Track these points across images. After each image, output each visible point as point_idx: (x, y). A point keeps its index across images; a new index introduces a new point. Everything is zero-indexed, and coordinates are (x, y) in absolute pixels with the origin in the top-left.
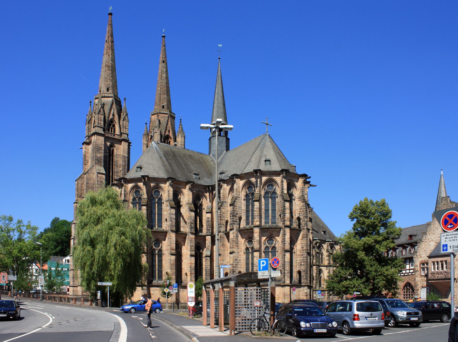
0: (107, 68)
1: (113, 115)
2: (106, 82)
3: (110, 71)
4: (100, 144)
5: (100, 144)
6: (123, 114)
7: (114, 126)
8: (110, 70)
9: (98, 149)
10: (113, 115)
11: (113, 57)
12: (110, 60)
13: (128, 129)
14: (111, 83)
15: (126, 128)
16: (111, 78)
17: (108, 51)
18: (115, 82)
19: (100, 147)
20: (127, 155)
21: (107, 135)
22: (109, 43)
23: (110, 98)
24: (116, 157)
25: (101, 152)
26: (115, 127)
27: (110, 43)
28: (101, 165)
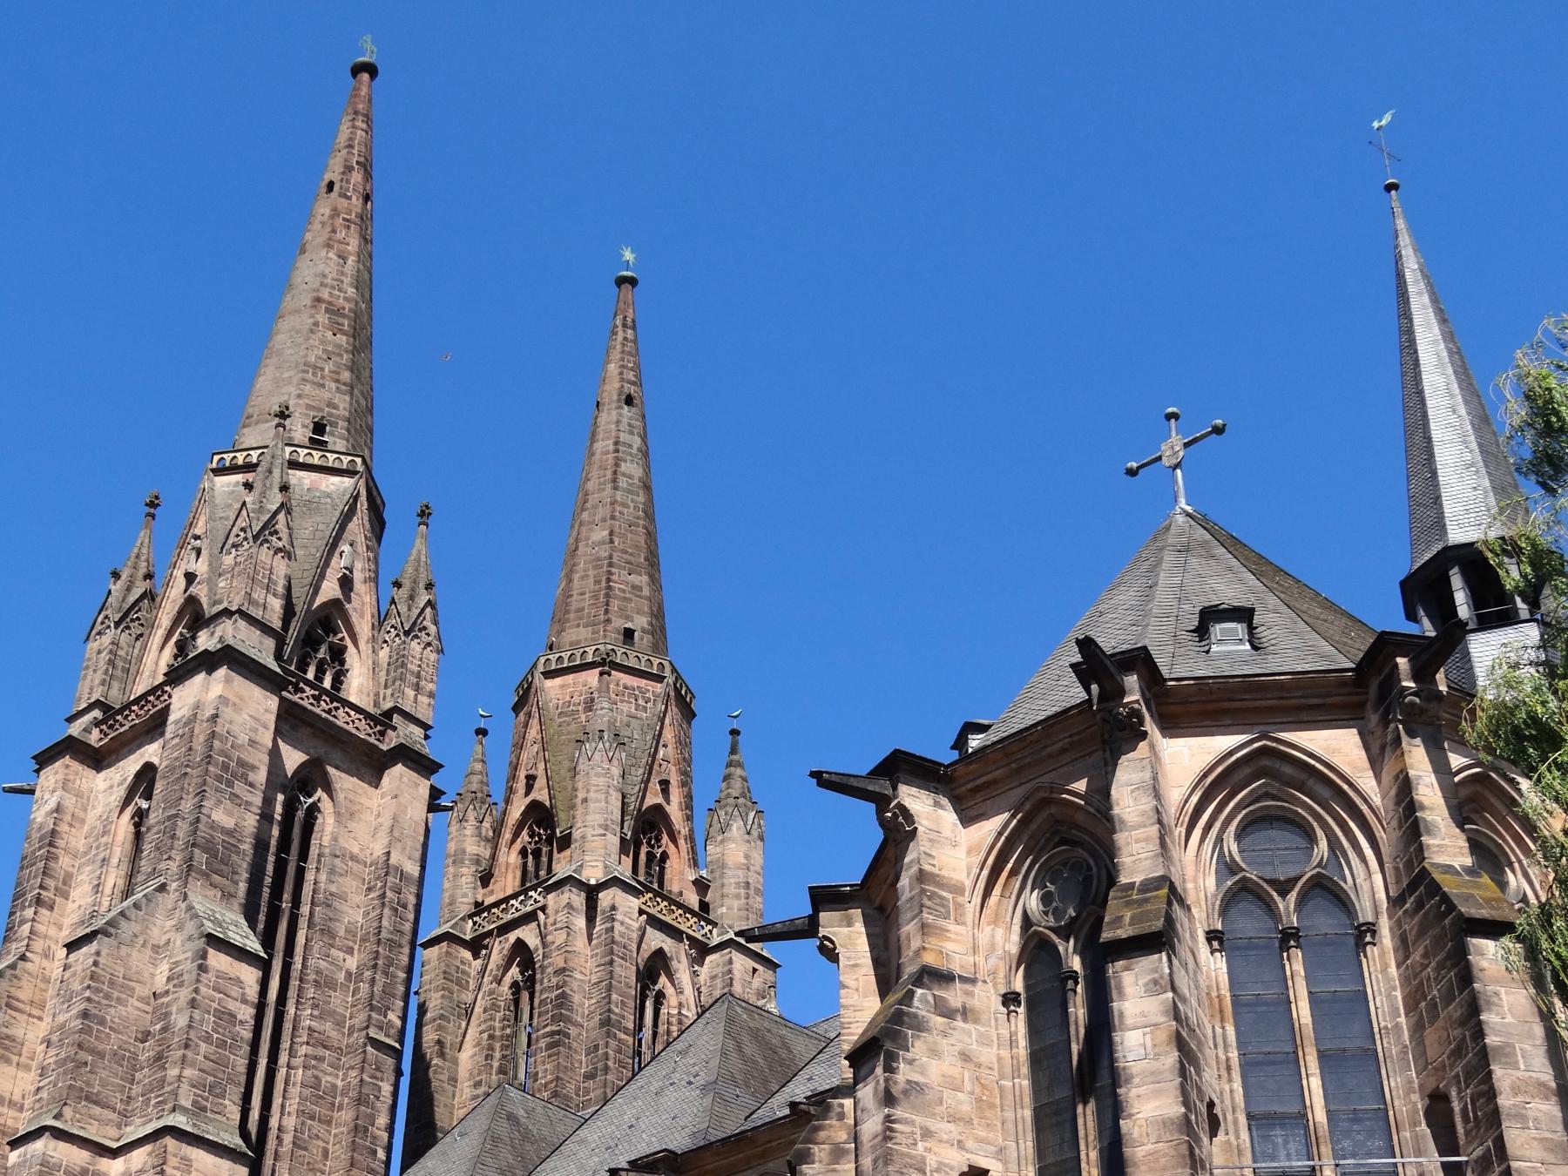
0: (322, 318)
1: (346, 583)
2: (308, 388)
3: (342, 339)
4: (243, 738)
5: (243, 738)
6: (412, 598)
7: (338, 654)
8: (344, 333)
9: (225, 767)
10: (346, 583)
11: (366, 276)
12: (347, 280)
13: (431, 695)
14: (343, 403)
15: (417, 688)
16: (346, 376)
17: (341, 234)
18: (363, 403)
19: (241, 763)
20: (413, 869)
21: (295, 698)
22: (349, 198)
23: (335, 480)
24: (332, 871)
25: (248, 797)
26: (342, 663)
27: (356, 202)
28: (227, 896)
